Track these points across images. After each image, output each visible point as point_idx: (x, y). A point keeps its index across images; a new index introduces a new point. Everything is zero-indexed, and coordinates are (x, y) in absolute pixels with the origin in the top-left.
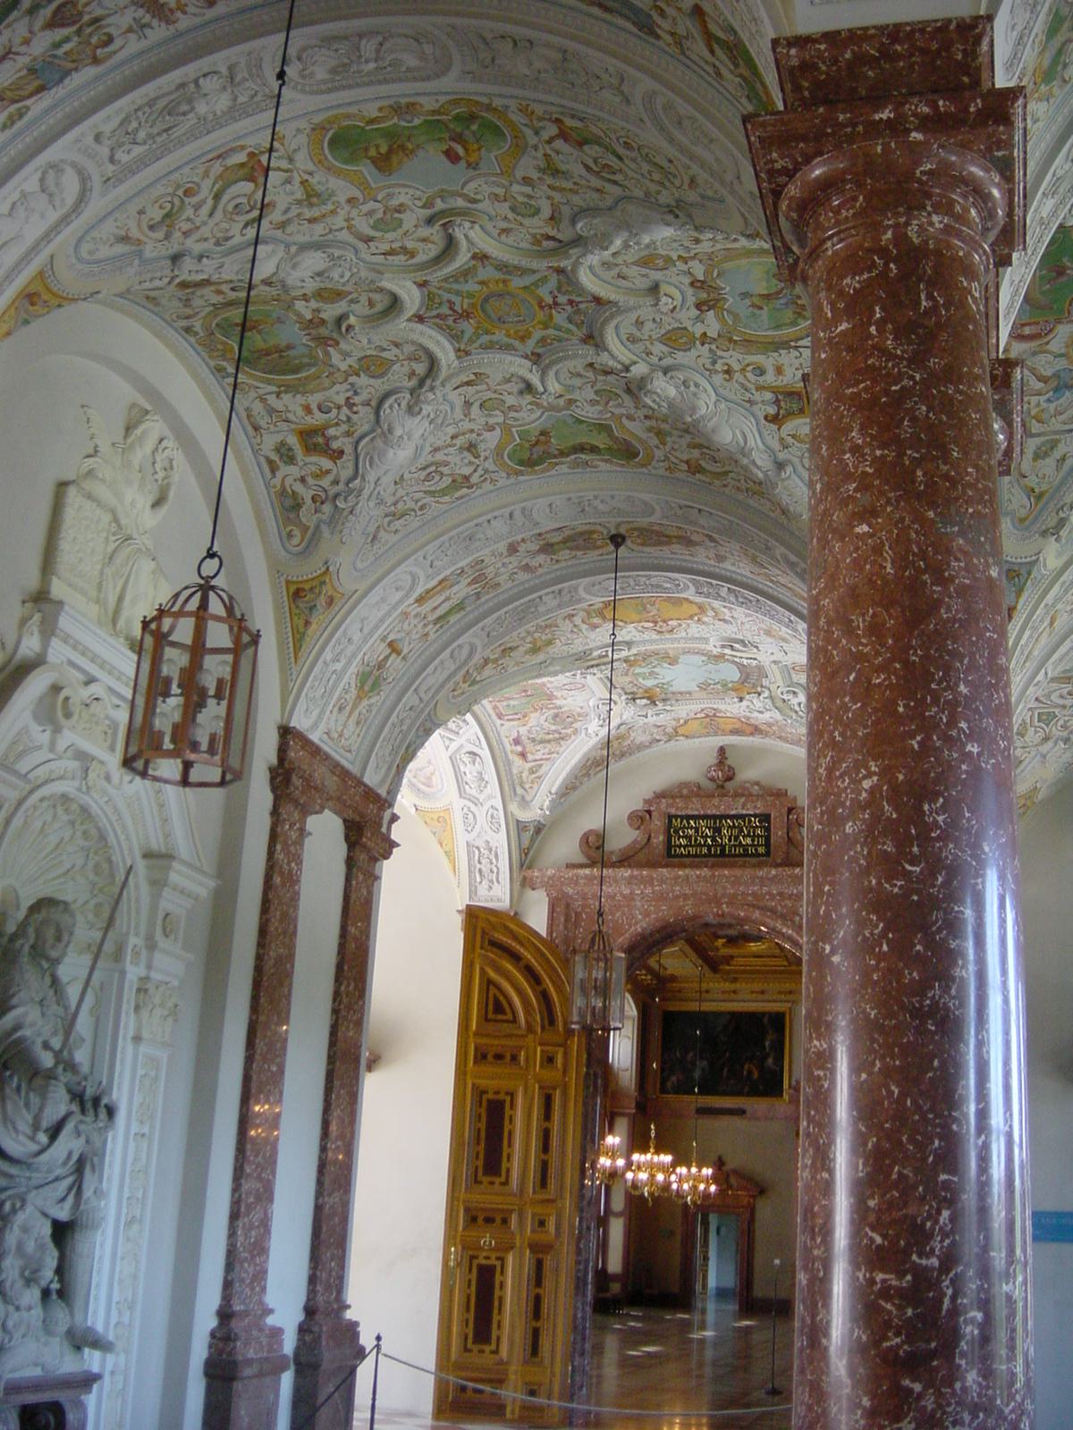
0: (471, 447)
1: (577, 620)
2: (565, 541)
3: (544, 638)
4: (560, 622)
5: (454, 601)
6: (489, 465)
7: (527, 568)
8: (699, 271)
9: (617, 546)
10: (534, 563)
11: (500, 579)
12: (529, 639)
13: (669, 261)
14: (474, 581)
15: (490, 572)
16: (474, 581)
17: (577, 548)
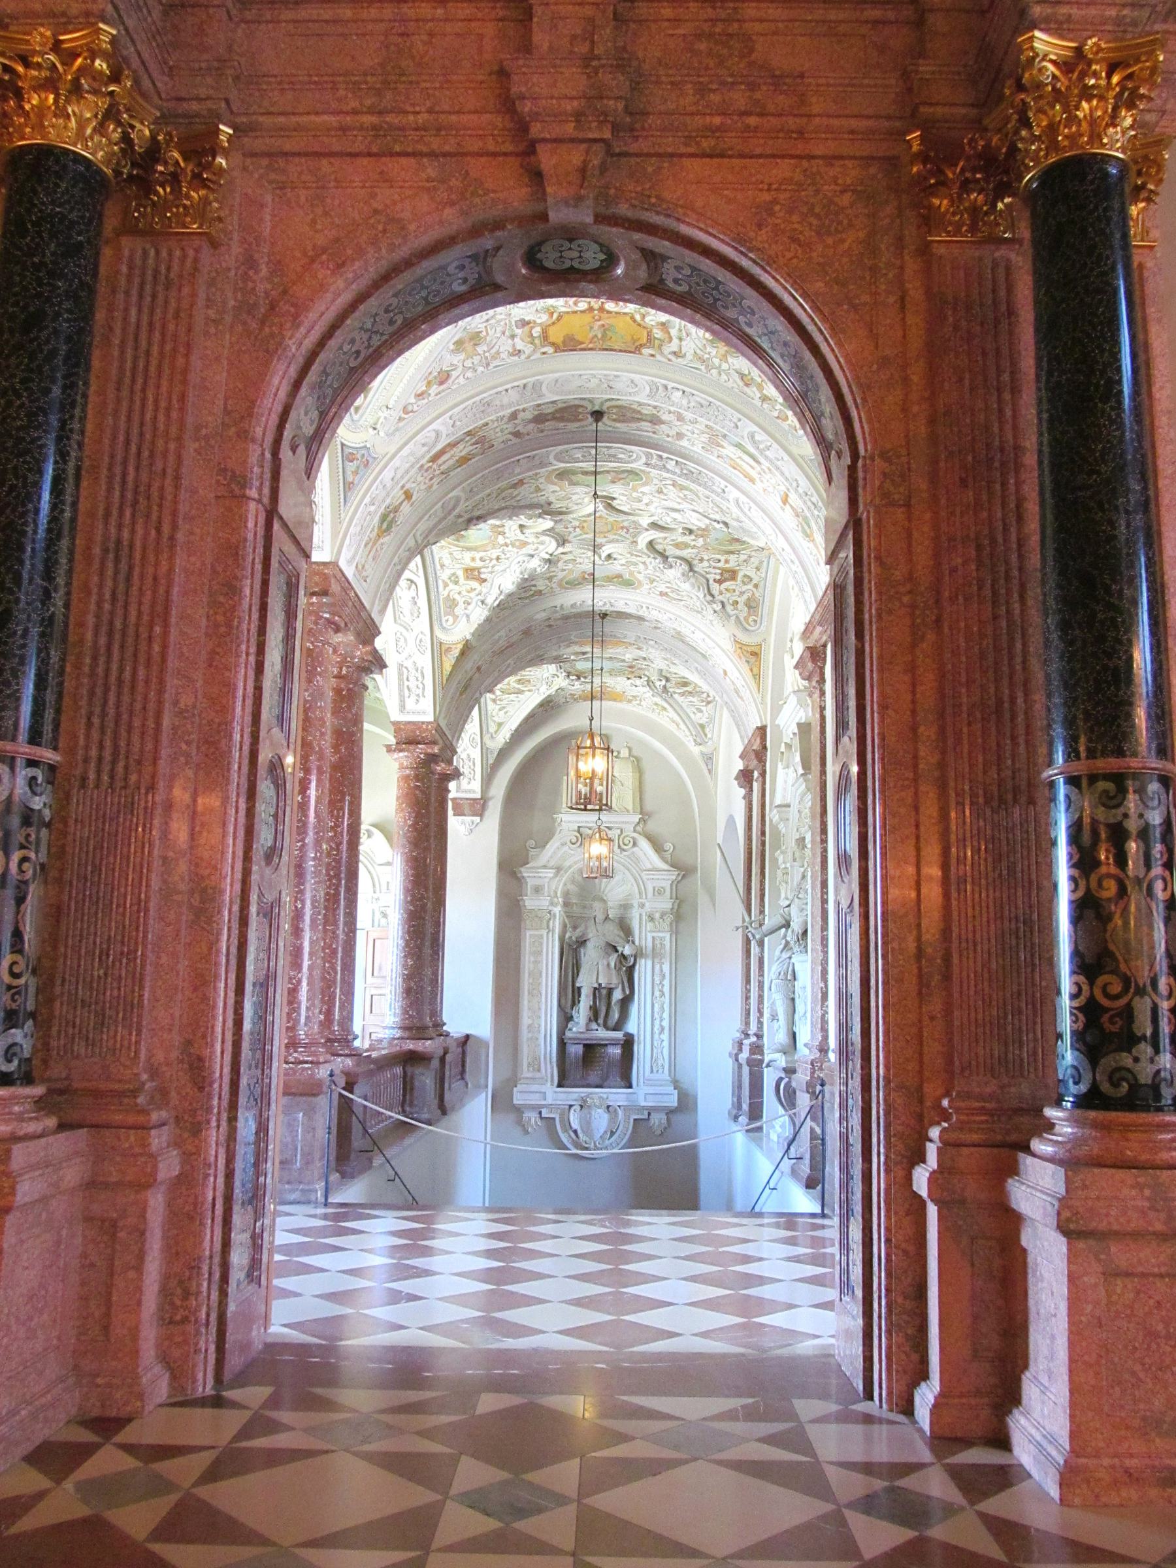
0: (660, 492)
1: (674, 346)
2: (640, 420)
3: (714, 352)
4: (689, 356)
5: (739, 453)
6: (656, 481)
7: (680, 418)
8: (501, 539)
9: (597, 421)
10: (672, 418)
11: (703, 427)
12: (725, 366)
13: (513, 545)
14: (719, 445)
15: (704, 438)
16: (719, 445)
17: (634, 411)
